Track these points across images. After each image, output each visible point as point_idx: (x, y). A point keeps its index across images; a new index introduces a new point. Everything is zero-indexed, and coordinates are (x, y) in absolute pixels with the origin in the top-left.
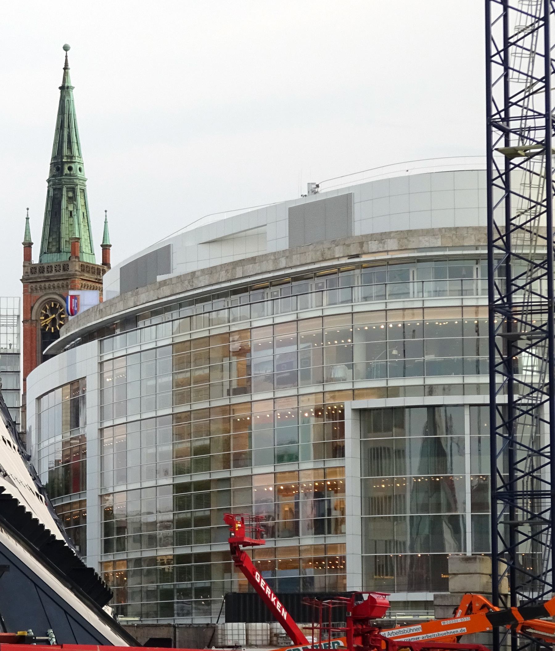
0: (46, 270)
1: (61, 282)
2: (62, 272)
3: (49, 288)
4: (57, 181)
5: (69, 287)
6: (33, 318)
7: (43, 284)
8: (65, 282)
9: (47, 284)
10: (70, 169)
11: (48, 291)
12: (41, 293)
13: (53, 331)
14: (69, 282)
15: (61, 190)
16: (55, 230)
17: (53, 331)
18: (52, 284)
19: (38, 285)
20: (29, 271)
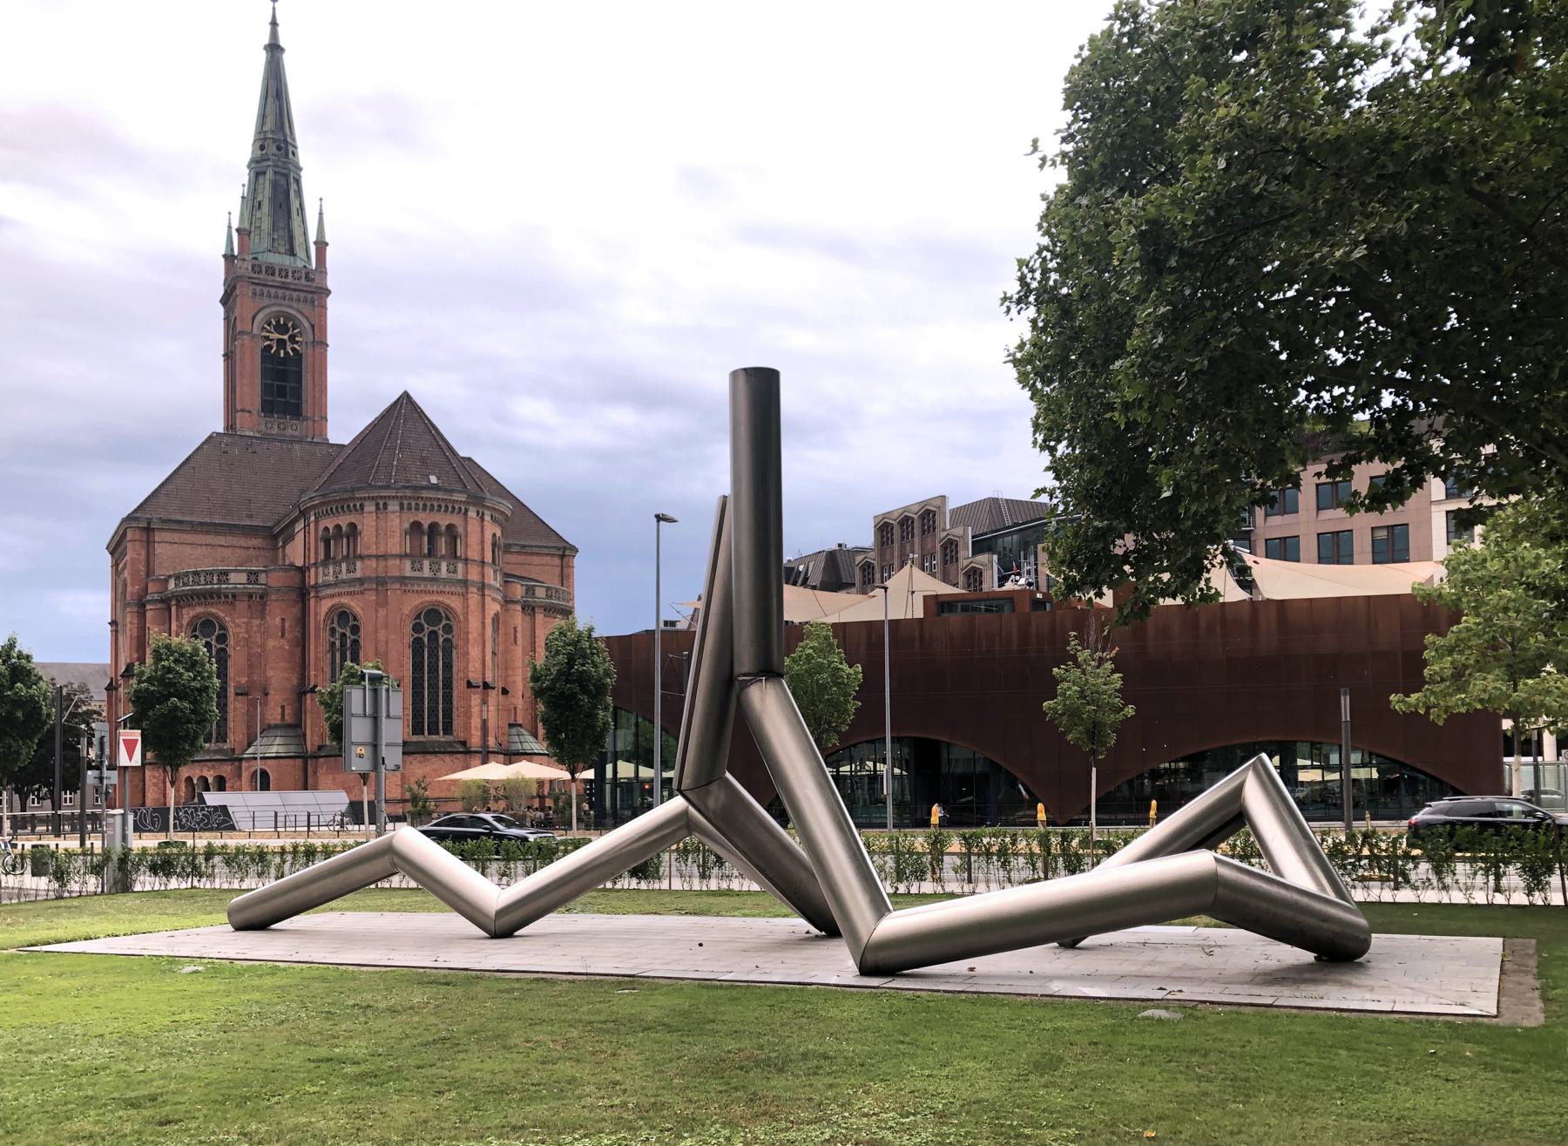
0: (277, 273)
1: (302, 295)
2: (303, 281)
3: (284, 298)
4: (280, 163)
5: (316, 303)
6: (255, 332)
7: (273, 291)
8: (309, 296)
9: (280, 292)
10: (293, 154)
11: (280, 301)
12: (266, 301)
13: (282, 355)
14: (316, 296)
15: (287, 176)
16: (282, 225)
17: (282, 355)
18: (288, 293)
19: (266, 290)
20: (250, 268)
